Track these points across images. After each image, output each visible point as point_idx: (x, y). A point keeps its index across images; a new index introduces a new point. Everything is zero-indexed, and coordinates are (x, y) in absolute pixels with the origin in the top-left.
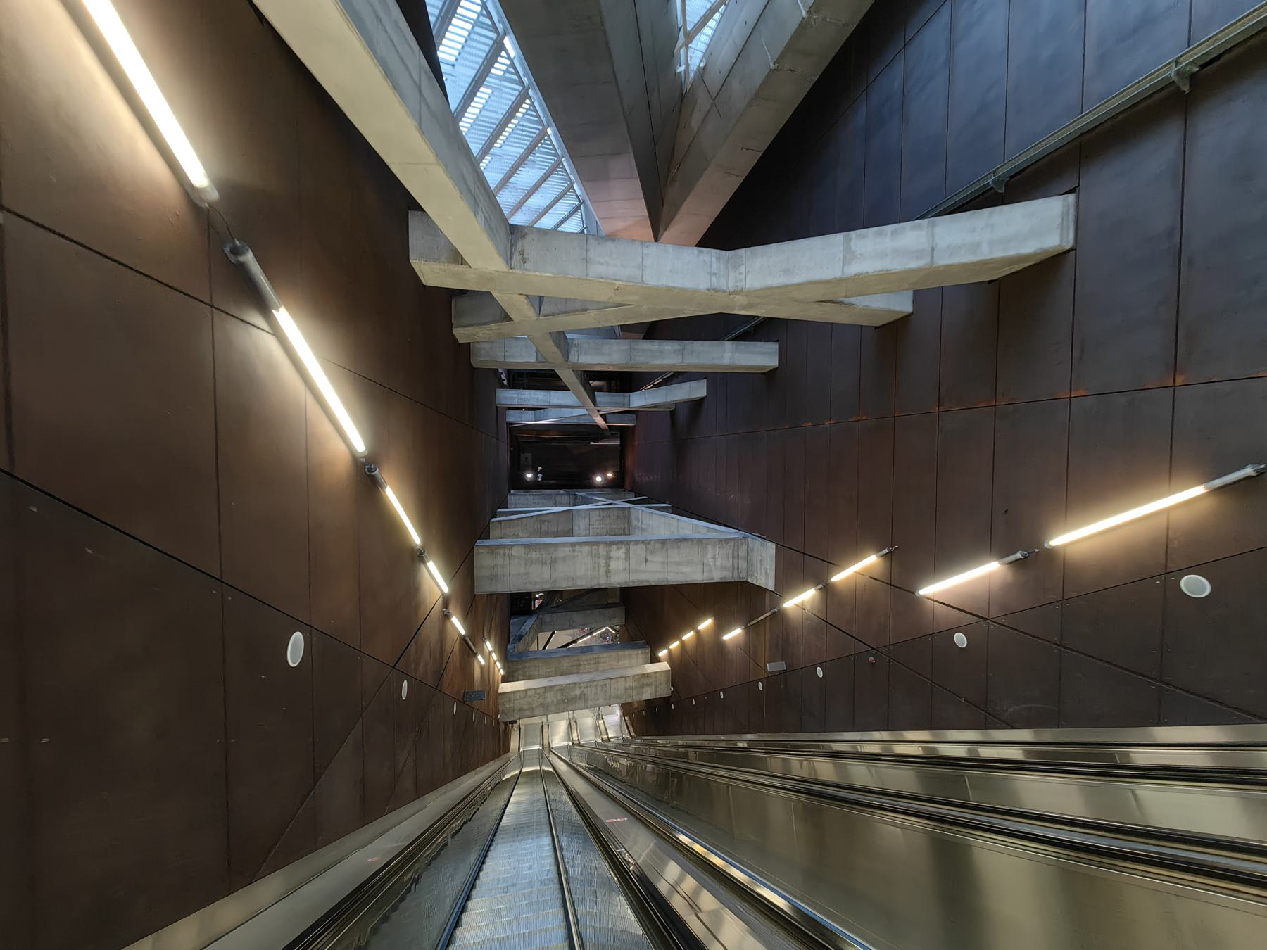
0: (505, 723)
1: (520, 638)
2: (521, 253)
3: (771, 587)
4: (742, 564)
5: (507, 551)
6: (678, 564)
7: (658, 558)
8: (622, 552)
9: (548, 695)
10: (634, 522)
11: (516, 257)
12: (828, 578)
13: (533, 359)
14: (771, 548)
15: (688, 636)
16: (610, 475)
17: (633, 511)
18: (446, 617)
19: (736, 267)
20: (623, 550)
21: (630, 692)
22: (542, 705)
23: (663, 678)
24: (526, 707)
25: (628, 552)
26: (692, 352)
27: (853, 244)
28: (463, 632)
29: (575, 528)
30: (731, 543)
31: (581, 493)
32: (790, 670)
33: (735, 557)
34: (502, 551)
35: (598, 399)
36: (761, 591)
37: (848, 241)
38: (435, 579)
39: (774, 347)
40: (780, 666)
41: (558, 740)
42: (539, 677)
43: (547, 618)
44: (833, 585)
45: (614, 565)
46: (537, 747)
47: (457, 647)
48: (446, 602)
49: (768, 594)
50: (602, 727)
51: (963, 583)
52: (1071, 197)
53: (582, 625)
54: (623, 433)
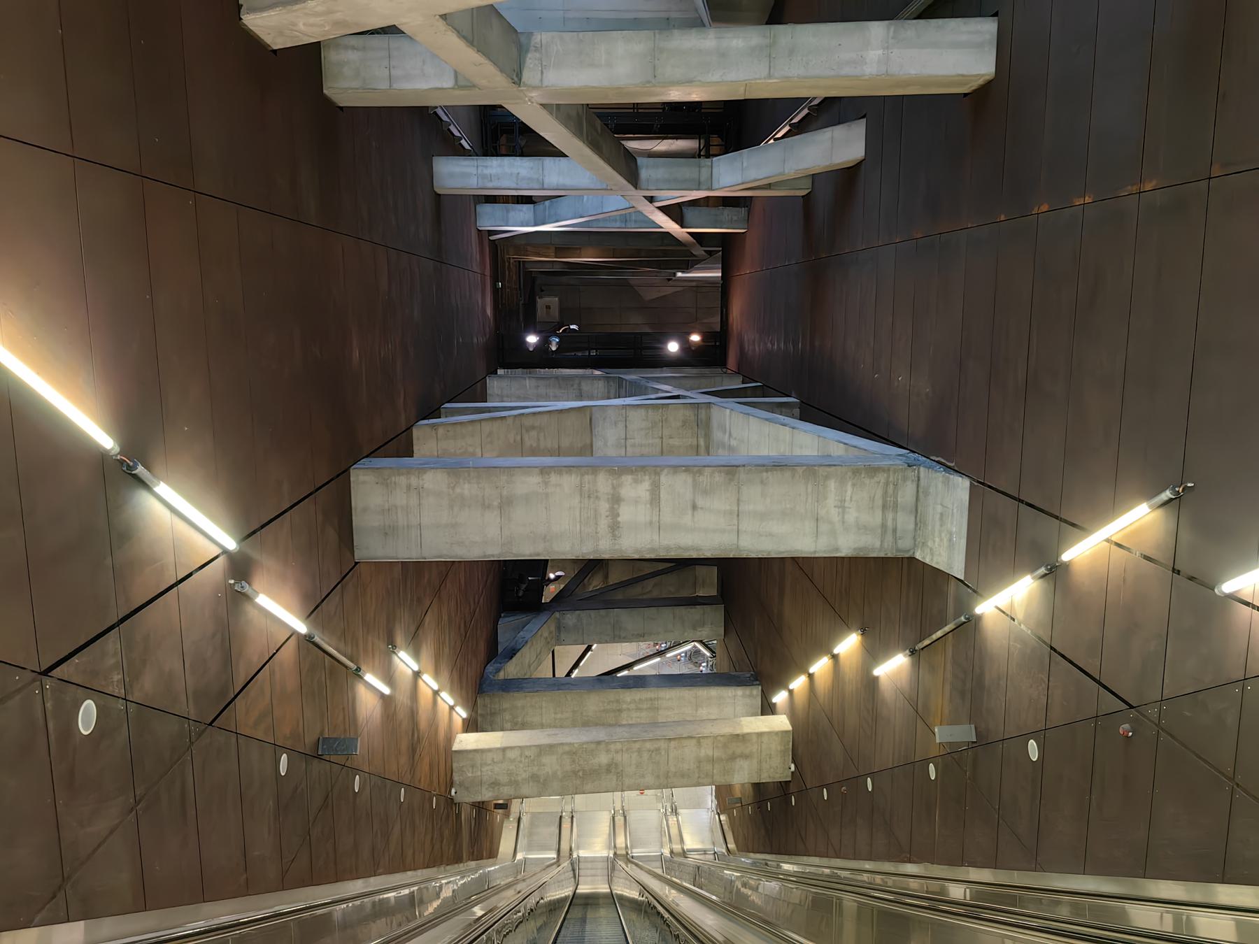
0: (480, 807)
1: (511, 653)
3: (958, 570)
4: (905, 521)
5: (414, 481)
6: (763, 516)
7: (721, 502)
9: (546, 760)
10: (717, 435)
12: (1058, 555)
13: (448, 83)
14: (962, 485)
15: (821, 666)
16: (695, 338)
17: (716, 413)
18: (234, 599)
21: (708, 767)
22: (534, 778)
23: (775, 746)
24: (504, 779)
26: (791, 52)
28: (302, 628)
29: (598, 444)
30: (881, 477)
31: (632, 376)
32: (982, 743)
33: (889, 505)
34: (403, 480)
35: (644, 174)
36: (940, 577)
38: (184, 519)
39: (987, 28)
40: (964, 733)
41: (595, 847)
42: (542, 726)
43: (570, 618)
44: (1066, 566)
47: (289, 652)
48: (240, 567)
49: (953, 582)
50: (674, 831)
53: (640, 636)
54: (724, 249)
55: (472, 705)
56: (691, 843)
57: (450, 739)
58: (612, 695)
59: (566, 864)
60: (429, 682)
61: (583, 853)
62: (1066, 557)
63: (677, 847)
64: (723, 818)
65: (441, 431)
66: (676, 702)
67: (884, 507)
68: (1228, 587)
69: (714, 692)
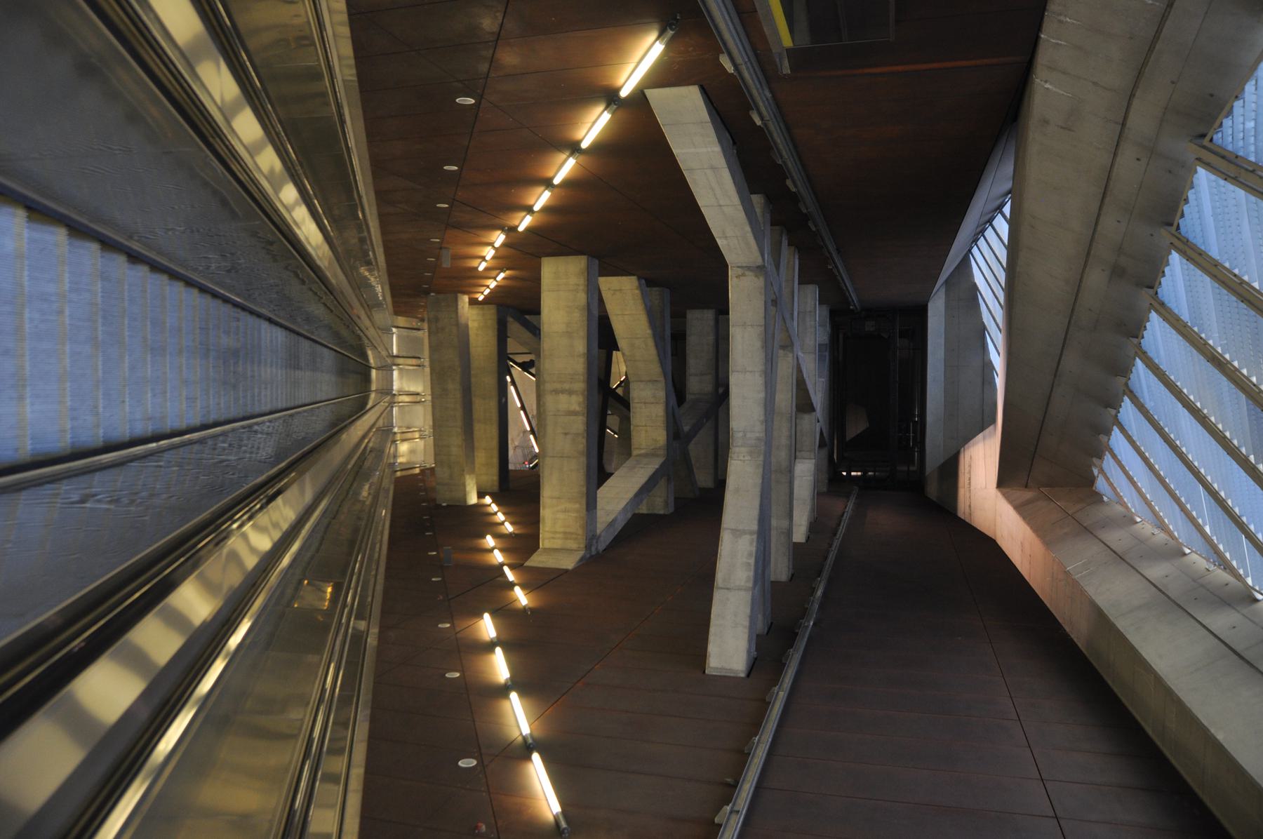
2: (743, 275)
3: (527, 564)
8: (576, 407)
11: (740, 271)
15: (501, 517)
19: (750, 453)
20: (577, 408)
25: (574, 413)
27: (748, 537)
37: (751, 533)
45: (563, 398)
46: (395, 352)
50: (409, 435)
51: (487, 627)
52: (743, 675)
55: (487, 300)
56: (404, 448)
57: (464, 293)
58: (494, 393)
59: (389, 361)
60: (493, 284)
61: (395, 374)
62: (517, 590)
63: (398, 437)
64: (417, 471)
65: (637, 292)
66: (486, 434)
67: (565, 533)
68: (487, 616)
69: (495, 461)
